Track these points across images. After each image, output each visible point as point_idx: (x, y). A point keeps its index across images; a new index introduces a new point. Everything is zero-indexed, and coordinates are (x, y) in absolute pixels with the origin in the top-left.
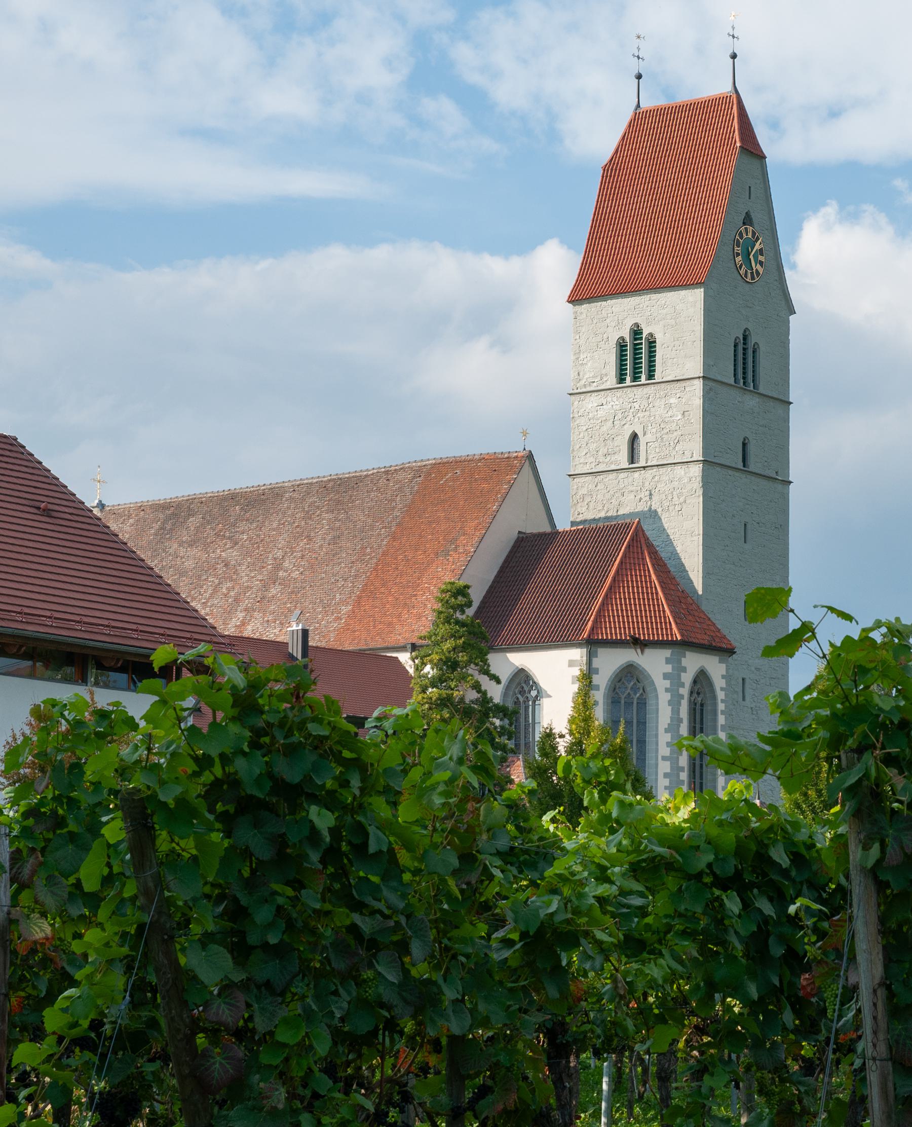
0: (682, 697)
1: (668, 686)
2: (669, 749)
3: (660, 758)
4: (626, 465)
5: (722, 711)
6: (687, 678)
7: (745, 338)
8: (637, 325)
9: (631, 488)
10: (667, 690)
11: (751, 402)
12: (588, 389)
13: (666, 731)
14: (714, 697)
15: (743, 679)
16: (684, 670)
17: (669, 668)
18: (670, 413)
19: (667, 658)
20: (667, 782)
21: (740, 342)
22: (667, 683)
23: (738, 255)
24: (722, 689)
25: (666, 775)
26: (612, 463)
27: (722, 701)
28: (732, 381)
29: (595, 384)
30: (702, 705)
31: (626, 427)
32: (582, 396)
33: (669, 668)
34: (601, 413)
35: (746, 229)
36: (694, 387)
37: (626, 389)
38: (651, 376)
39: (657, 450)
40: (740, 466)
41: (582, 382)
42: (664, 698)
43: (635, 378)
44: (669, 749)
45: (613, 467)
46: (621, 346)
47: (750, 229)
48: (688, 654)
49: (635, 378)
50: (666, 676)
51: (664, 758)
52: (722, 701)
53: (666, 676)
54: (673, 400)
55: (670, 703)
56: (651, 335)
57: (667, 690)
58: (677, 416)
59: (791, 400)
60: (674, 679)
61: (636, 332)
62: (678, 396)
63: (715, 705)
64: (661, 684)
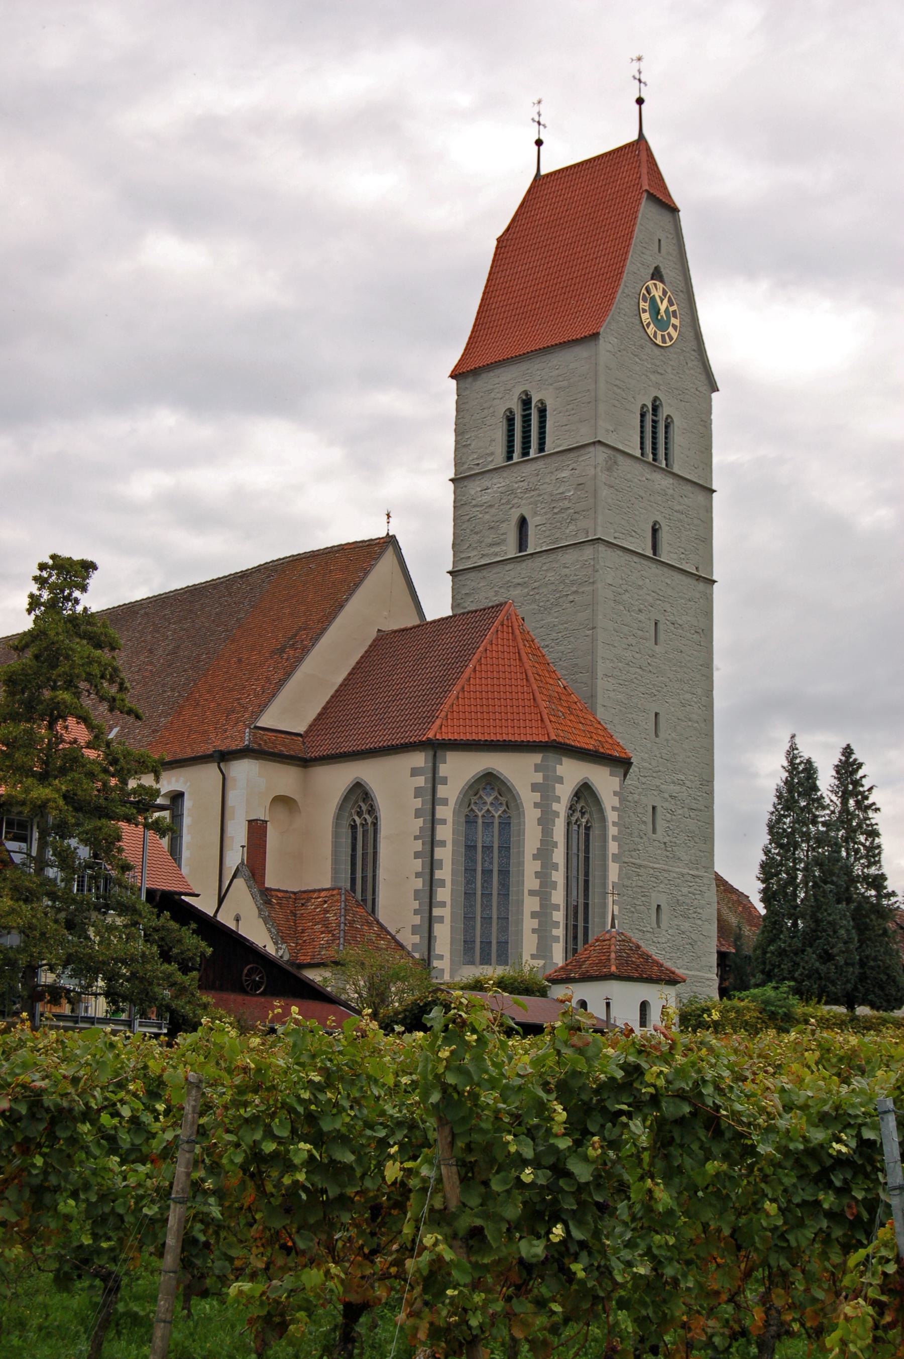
0: (557, 814)
1: (538, 800)
2: (538, 880)
3: (526, 893)
5: (613, 836)
6: (565, 792)
7: (655, 409)
8: (526, 393)
10: (536, 805)
11: (663, 482)
13: (535, 857)
14: (603, 819)
15: (654, 808)
16: (560, 780)
17: (539, 778)
19: (536, 765)
20: (535, 924)
21: (648, 411)
22: (537, 797)
23: (644, 311)
24: (614, 809)
25: (534, 915)
27: (614, 824)
28: (638, 453)
30: (587, 828)
33: (539, 778)
35: (655, 285)
36: (589, 455)
38: (541, 449)
40: (650, 553)
42: (531, 815)
43: (525, 452)
44: (538, 880)
47: (660, 285)
48: (565, 760)
49: (525, 452)
50: (535, 787)
51: (532, 893)
52: (614, 824)
53: (535, 787)
55: (540, 822)
56: (541, 401)
57: (536, 805)
59: (714, 488)
60: (545, 790)
62: (571, 467)
63: (604, 828)
64: (528, 798)
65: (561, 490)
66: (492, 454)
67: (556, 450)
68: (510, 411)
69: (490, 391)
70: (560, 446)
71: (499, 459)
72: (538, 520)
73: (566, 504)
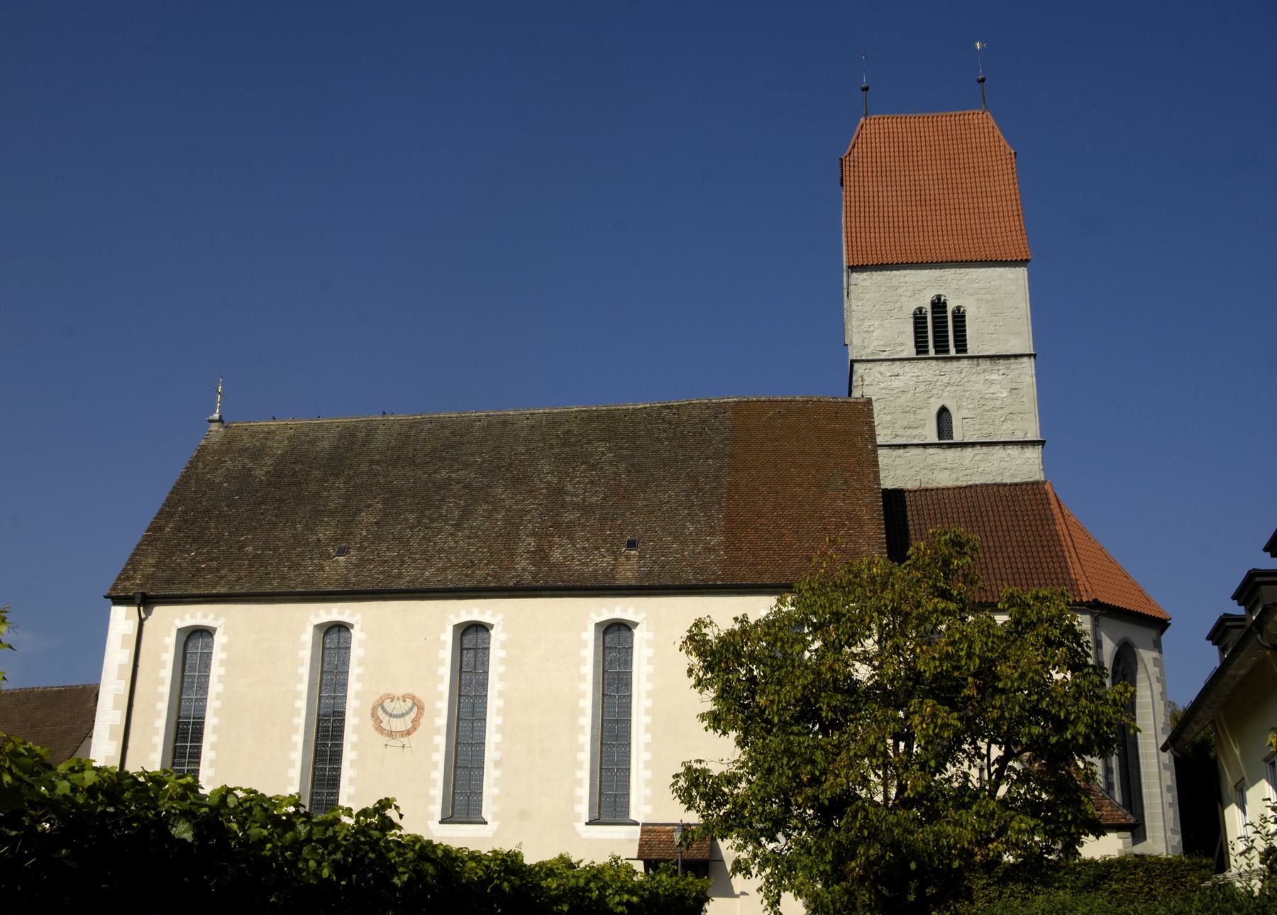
4: (936, 440)
9: (943, 465)
12: (876, 357)
18: (992, 390)
26: (914, 437)
29: (885, 353)
31: (932, 400)
32: (870, 365)
34: (896, 383)
36: (1023, 365)
37: (930, 361)
39: (977, 427)
41: (869, 350)
45: (915, 441)
46: (919, 319)
54: (994, 377)
56: (958, 308)
58: (1001, 393)
61: (939, 305)
62: (1002, 372)
65: (992, 390)
66: (901, 344)
67: (980, 354)
68: (920, 309)
69: (896, 288)
70: (986, 351)
71: (910, 350)
72: (964, 413)
73: (998, 403)
